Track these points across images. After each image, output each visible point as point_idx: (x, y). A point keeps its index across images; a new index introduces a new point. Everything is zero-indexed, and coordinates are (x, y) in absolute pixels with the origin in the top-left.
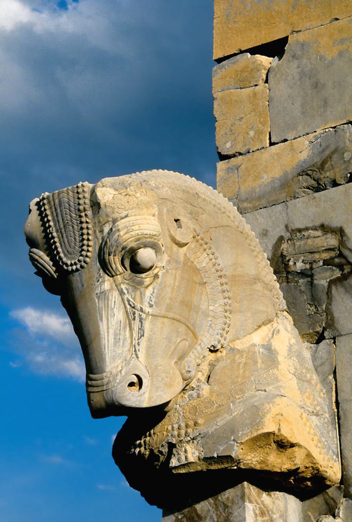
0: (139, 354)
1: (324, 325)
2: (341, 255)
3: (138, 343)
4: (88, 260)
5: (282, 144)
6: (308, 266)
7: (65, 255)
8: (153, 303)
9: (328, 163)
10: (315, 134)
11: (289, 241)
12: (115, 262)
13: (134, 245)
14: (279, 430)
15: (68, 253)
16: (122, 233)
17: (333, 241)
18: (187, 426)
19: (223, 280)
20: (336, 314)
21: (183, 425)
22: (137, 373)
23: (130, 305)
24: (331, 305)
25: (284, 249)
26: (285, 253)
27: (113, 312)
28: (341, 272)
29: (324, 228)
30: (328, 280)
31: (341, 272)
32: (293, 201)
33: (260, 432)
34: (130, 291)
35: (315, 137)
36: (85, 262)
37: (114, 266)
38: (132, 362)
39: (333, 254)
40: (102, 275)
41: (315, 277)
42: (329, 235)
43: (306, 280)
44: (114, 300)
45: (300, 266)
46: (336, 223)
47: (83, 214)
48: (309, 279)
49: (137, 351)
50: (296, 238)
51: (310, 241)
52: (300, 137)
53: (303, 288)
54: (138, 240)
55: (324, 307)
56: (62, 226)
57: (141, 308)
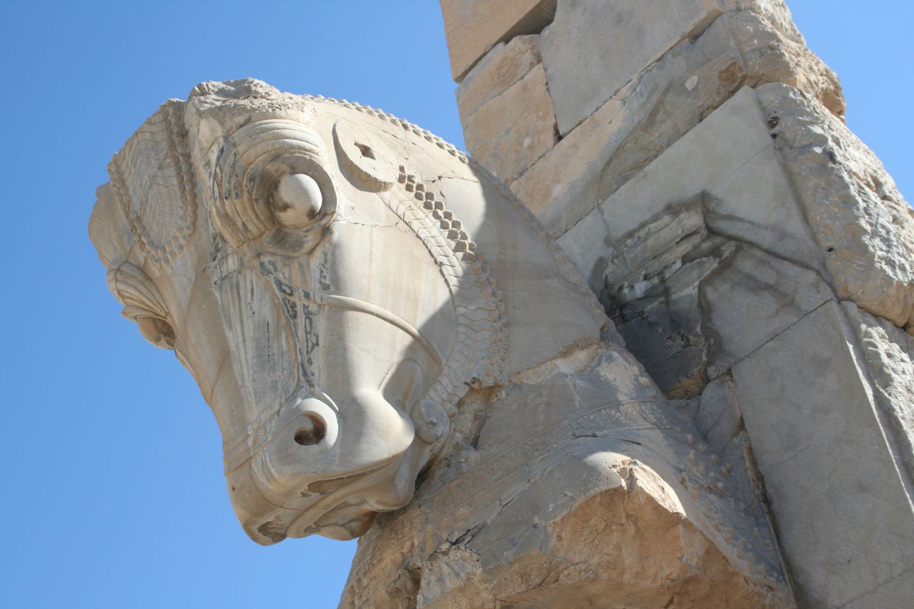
0: (315, 379)
1: (704, 358)
2: (712, 232)
8: (328, 282)
11: (616, 261)
17: (693, 220)
23: (284, 291)
24: (710, 320)
25: (609, 277)
26: (611, 280)
27: (251, 308)
28: (718, 260)
29: (673, 209)
30: (696, 284)
31: (718, 260)
34: (279, 265)
39: (696, 240)
40: (220, 246)
41: (673, 290)
42: (683, 215)
44: (249, 284)
45: (641, 288)
46: (692, 190)
48: (662, 299)
49: (309, 374)
50: (625, 249)
51: (651, 242)
52: (605, 102)
55: (698, 329)
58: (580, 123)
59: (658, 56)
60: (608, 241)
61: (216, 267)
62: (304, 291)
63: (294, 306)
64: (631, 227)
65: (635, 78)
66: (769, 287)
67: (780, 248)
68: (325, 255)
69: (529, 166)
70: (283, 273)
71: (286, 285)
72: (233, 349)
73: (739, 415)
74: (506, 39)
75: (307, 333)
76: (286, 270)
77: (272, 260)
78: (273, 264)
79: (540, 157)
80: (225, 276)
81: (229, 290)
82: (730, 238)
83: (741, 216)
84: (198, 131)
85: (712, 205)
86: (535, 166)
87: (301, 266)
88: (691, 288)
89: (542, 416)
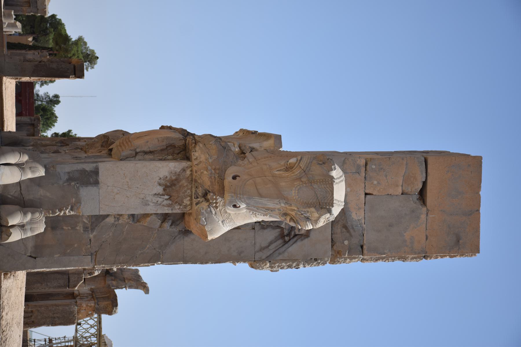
5: (364, 202)
9: (345, 230)
10: (364, 223)
20: (266, 231)
24: (271, 228)
28: (286, 235)
30: (284, 227)
34: (279, 211)
35: (362, 224)
52: (364, 214)
58: (365, 203)
59: (365, 235)
63: (268, 210)
65: (364, 226)
66: (269, 246)
67: (277, 252)
69: (366, 182)
72: (262, 199)
73: (242, 228)
74: (425, 184)
79: (365, 186)
82: (290, 240)
83: (294, 245)
84: (318, 213)
85: (303, 237)
86: (364, 183)
87: (277, 215)
88: (284, 225)
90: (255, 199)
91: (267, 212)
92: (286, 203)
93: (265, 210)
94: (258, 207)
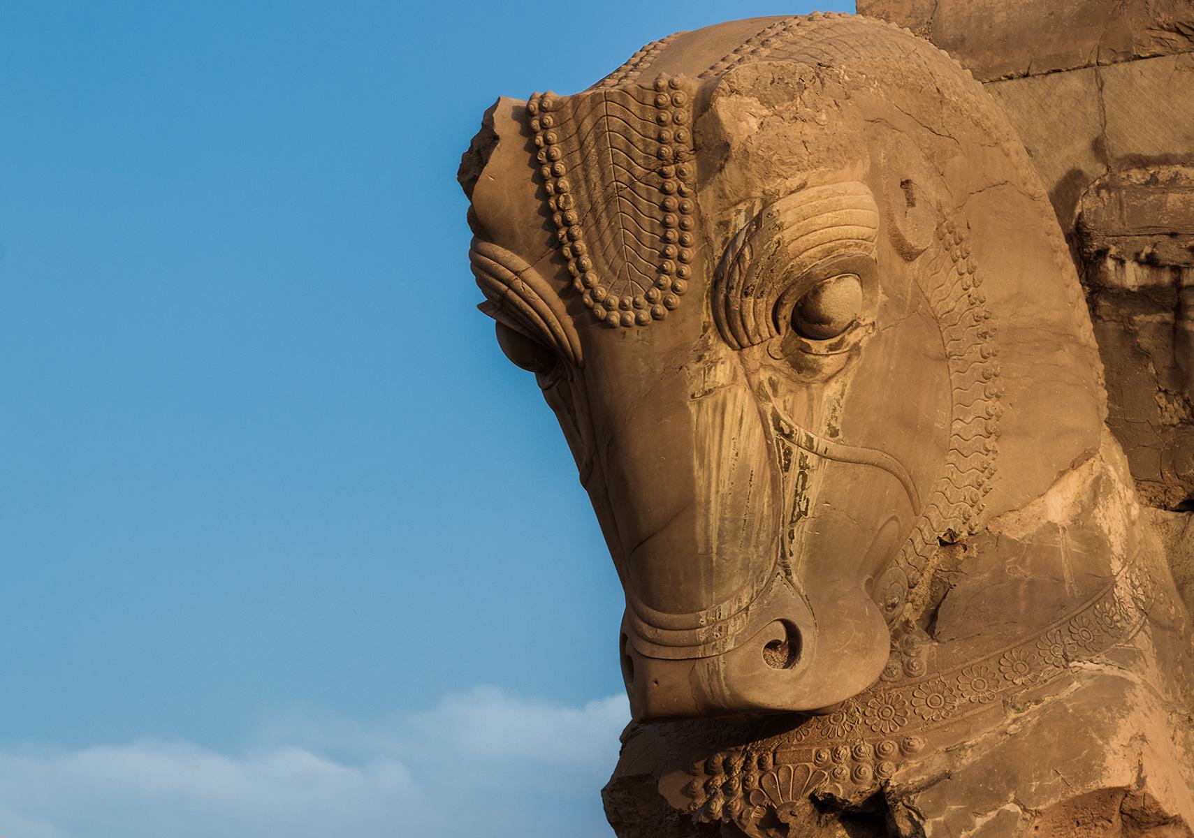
0: (791, 560)
3: (791, 533)
4: (675, 300)
6: (1166, 278)
7: (604, 280)
12: (756, 312)
13: (819, 268)
14: (1141, 781)
15: (614, 275)
16: (786, 235)
18: (879, 754)
19: (989, 345)
21: (867, 749)
22: (790, 616)
32: (1122, 67)
33: (1093, 786)
34: (782, 389)
36: (666, 304)
37: (751, 323)
38: (775, 584)
40: (711, 342)
43: (1157, 318)
47: (670, 170)
48: (1168, 317)
49: (788, 555)
53: (1145, 341)
54: (829, 252)
56: (598, 194)
57: (810, 440)
60: (1098, 147)
61: (698, 371)
62: (807, 435)
63: (788, 453)
64: (1147, 151)
68: (845, 385)
70: (784, 402)
71: (784, 421)
75: (796, 494)
76: (789, 398)
77: (774, 378)
78: (773, 385)
80: (710, 390)
81: (710, 412)
89: (1023, 605)
90: (708, 541)
91: (803, 458)
92: (700, 358)
93: (795, 469)
94: (777, 511)
